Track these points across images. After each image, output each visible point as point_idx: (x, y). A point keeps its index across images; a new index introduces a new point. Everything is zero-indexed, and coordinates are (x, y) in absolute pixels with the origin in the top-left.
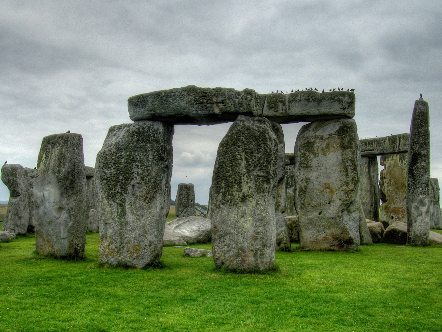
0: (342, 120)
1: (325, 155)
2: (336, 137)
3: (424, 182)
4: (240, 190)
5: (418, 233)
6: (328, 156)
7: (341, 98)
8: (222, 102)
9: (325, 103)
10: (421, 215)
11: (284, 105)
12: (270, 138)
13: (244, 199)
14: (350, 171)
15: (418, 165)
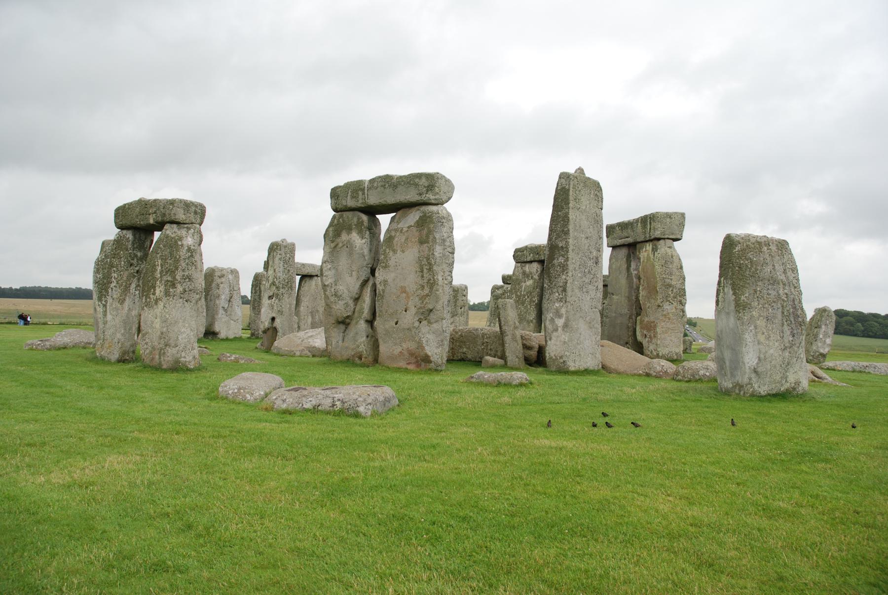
0: (423, 208)
1: (403, 252)
2: (414, 229)
3: (561, 284)
4: (154, 294)
5: (552, 355)
6: (406, 253)
7: (417, 180)
8: (155, 213)
9: (400, 188)
10: (556, 330)
11: (364, 194)
12: (182, 245)
13: (157, 301)
14: (425, 271)
15: (555, 261)
